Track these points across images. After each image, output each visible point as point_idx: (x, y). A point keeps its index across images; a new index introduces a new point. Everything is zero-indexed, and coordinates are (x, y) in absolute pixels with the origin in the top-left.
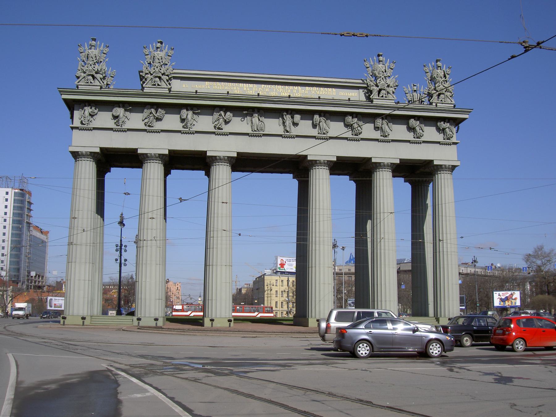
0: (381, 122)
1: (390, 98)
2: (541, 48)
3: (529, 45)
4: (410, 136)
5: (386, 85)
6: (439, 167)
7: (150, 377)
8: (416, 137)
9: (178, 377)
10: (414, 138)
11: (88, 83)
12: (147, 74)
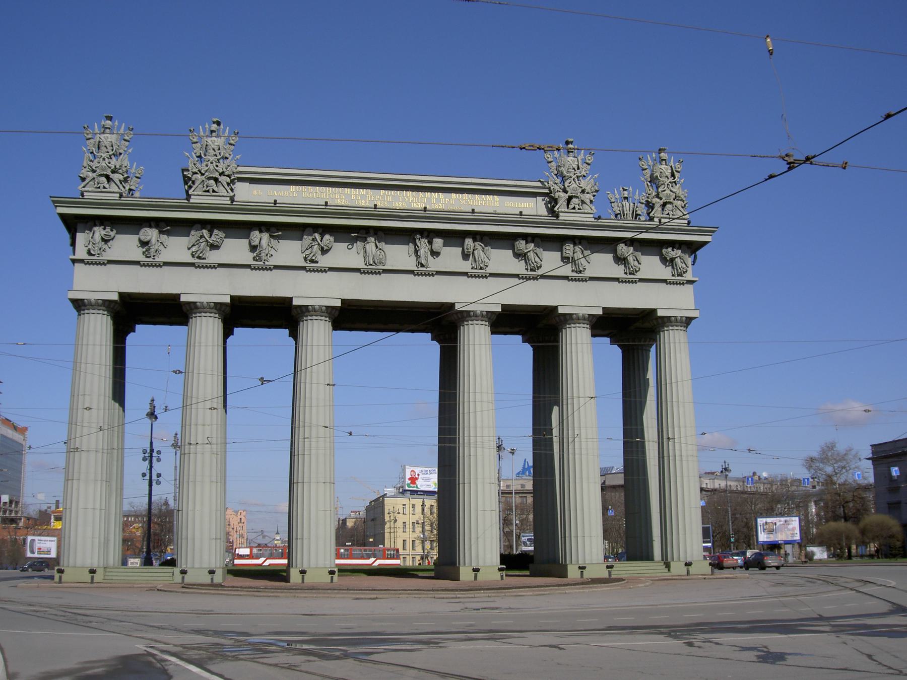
0: (572, 250)
1: (586, 211)
2: (811, 163)
3: (794, 160)
4: (618, 271)
5: (580, 190)
6: (666, 320)
7: (218, 663)
8: (628, 272)
9: (263, 663)
10: (626, 273)
11: (99, 188)
12: (196, 173)
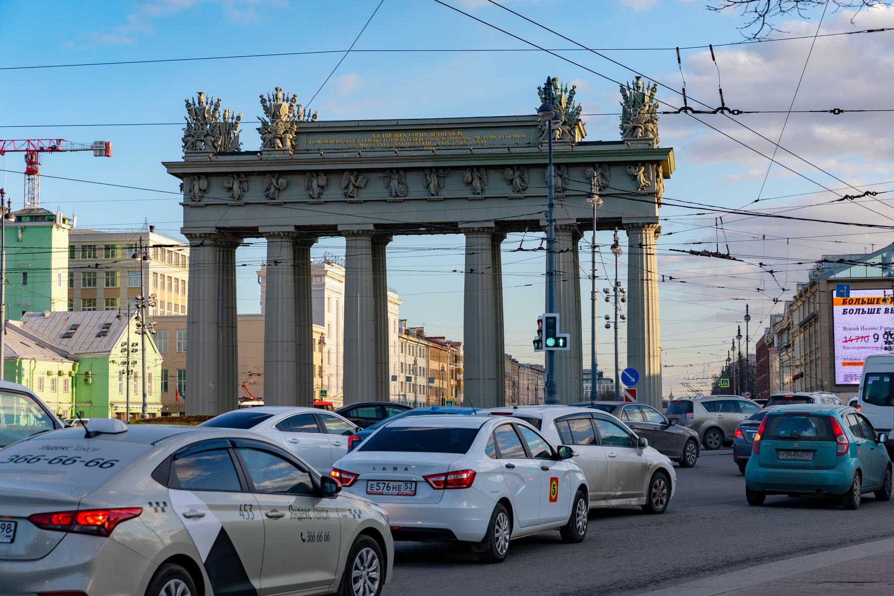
11: (197, 150)
